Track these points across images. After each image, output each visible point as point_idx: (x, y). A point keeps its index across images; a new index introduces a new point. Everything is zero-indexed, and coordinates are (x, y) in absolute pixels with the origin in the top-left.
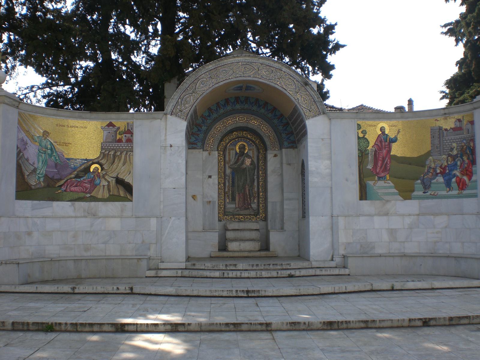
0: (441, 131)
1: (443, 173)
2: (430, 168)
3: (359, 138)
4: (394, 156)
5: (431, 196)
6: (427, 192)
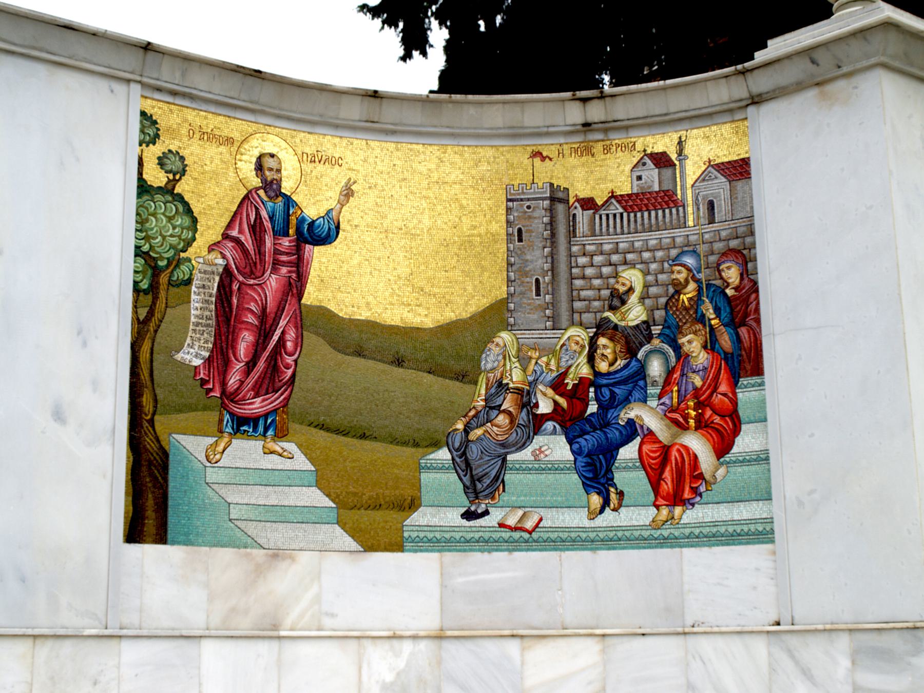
0: (560, 208)
1: (570, 421)
2: (501, 386)
3: (144, 188)
4: (323, 313)
5: (506, 534)
6: (486, 513)
